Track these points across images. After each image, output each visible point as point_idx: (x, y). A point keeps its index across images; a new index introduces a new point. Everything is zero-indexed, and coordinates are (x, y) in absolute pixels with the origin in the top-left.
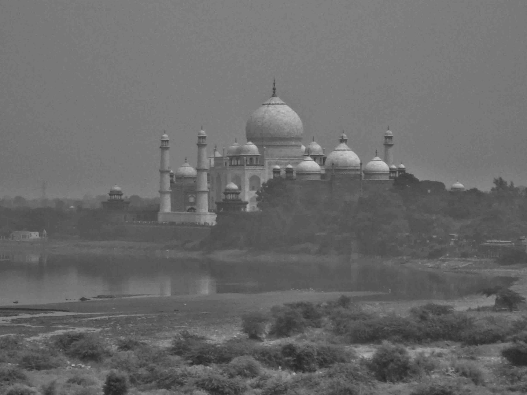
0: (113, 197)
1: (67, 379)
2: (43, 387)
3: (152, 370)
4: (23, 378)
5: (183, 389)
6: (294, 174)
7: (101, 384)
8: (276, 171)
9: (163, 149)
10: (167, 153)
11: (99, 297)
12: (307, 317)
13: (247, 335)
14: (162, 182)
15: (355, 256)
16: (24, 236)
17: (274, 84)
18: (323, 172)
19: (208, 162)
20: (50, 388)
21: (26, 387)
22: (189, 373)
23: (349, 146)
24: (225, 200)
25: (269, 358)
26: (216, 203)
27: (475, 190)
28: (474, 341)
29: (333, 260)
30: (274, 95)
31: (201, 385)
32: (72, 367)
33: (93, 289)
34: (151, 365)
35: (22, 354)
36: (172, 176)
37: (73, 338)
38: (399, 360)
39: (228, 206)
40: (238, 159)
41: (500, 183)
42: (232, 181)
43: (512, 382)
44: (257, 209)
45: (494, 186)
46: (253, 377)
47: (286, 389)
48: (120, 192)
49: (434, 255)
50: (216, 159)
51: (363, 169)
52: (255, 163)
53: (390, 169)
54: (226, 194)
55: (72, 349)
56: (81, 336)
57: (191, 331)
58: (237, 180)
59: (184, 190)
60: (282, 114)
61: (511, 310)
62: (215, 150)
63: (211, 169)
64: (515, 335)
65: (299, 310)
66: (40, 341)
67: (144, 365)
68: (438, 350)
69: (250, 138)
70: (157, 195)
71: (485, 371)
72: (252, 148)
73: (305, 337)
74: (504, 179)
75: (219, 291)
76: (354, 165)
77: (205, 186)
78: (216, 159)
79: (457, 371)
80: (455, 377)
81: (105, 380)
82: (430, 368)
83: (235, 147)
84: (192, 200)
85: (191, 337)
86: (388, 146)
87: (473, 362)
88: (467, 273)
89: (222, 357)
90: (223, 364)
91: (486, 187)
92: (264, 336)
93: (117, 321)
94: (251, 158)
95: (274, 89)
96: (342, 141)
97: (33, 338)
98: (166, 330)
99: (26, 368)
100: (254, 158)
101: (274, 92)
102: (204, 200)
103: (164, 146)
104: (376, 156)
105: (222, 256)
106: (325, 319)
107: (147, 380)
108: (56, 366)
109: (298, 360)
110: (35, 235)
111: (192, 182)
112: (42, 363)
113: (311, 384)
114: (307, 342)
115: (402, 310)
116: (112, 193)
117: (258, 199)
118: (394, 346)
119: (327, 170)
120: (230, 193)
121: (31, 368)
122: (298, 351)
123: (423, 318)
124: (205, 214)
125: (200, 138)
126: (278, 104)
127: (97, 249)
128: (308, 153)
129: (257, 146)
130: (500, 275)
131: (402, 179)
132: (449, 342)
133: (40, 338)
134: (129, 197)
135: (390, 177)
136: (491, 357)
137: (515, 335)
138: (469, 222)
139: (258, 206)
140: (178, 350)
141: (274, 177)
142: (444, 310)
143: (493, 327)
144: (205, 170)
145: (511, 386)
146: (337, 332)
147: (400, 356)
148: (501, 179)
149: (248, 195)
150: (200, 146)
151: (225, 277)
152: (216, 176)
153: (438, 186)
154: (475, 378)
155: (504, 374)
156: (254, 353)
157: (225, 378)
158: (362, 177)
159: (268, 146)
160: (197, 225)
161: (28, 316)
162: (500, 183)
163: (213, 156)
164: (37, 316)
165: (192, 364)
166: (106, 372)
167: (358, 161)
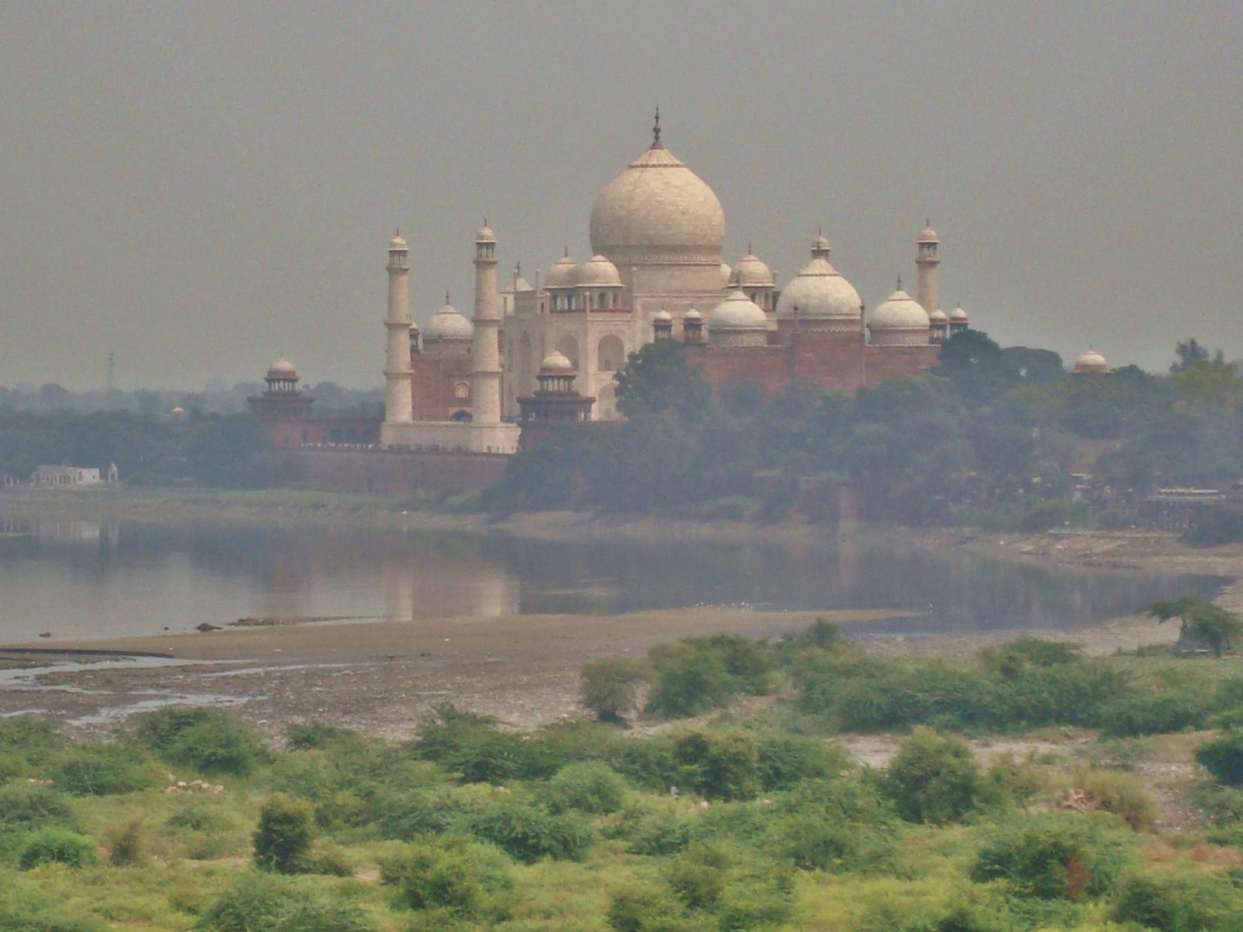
0: (276, 387)
1: (166, 816)
2: (110, 834)
3: (369, 794)
4: (61, 814)
5: (443, 840)
6: (704, 332)
7: (249, 826)
8: (661, 326)
10: (403, 279)
11: (241, 622)
13: (594, 714)
14: (390, 351)
15: (847, 526)
16: (65, 479)
17: (657, 118)
18: (773, 327)
19: (500, 304)
20: (128, 838)
21: (72, 835)
22: (456, 803)
23: (835, 265)
24: (542, 394)
25: (646, 768)
26: (520, 400)
27: (1132, 369)
28: (1127, 727)
29: (796, 534)
30: (656, 145)
31: (485, 831)
32: (178, 787)
34: (367, 783)
35: (65, 756)
36: (414, 335)
37: (182, 720)
38: (953, 772)
40: (571, 297)
41: (1191, 352)
42: (557, 349)
43: (1219, 823)
44: (616, 415)
45: (1179, 360)
46: (607, 811)
47: (685, 840)
48: (292, 373)
49: (1034, 524)
50: (519, 296)
51: (866, 321)
52: (611, 307)
53: (932, 320)
54: (541, 378)
55: (179, 746)
56: (199, 715)
57: (460, 704)
58: (570, 346)
59: (442, 370)
60: (676, 190)
61: (1217, 655)
62: (517, 275)
63: (507, 318)
64: (1226, 713)
65: (716, 654)
66: (103, 727)
67: (350, 783)
68: (1044, 748)
69: (601, 247)
70: (381, 382)
71: (1155, 798)
72: (605, 270)
73: (726, 717)
74: (1200, 343)
75: (524, 609)
76: (845, 310)
77: (492, 359)
78: (519, 296)
79: (1090, 796)
80: (1083, 813)
81: (259, 819)
82: (1026, 791)
83: (563, 267)
84: (461, 393)
85: (460, 717)
86: (925, 265)
87: (1124, 778)
88: (1115, 565)
90: (538, 781)
91: (1158, 360)
92: (633, 714)
93: (284, 679)
94: (603, 293)
95: (657, 131)
96: (818, 253)
97: (86, 720)
98: (403, 702)
99: (71, 789)
100: (610, 295)
101: (657, 138)
102: (491, 394)
103: (396, 264)
104: (899, 289)
105: (536, 525)
106: (778, 675)
107: (356, 820)
108: (141, 786)
109: (713, 773)
110: (90, 476)
112: (112, 778)
113: (745, 828)
115: (961, 653)
116: (274, 376)
117: (618, 392)
118: (940, 740)
119: (780, 322)
120: (553, 378)
121: (84, 791)
122: (714, 751)
123: (1009, 672)
124: (492, 427)
125: (480, 245)
126: (666, 166)
127: (237, 508)
128: (737, 282)
129: (617, 265)
130: (1194, 570)
131: (960, 345)
134: (312, 386)
135: (932, 340)
136: (1170, 765)
137: (1226, 713)
139: (619, 407)
140: (431, 747)
141: (656, 339)
142: (1058, 654)
144: (494, 321)
146: (807, 704)
147: (952, 760)
148: (1193, 343)
149: (596, 382)
150: (482, 264)
151: (540, 575)
152: (519, 337)
153: (1049, 359)
154: (1134, 815)
155: (1202, 805)
156: (609, 755)
157: (541, 814)
158: (863, 341)
159: (642, 266)
160: (474, 454)
161: (74, 667)
162: (1191, 352)
163: (510, 288)
164: (97, 666)
165: (463, 781)
166: (258, 799)
167: (856, 301)
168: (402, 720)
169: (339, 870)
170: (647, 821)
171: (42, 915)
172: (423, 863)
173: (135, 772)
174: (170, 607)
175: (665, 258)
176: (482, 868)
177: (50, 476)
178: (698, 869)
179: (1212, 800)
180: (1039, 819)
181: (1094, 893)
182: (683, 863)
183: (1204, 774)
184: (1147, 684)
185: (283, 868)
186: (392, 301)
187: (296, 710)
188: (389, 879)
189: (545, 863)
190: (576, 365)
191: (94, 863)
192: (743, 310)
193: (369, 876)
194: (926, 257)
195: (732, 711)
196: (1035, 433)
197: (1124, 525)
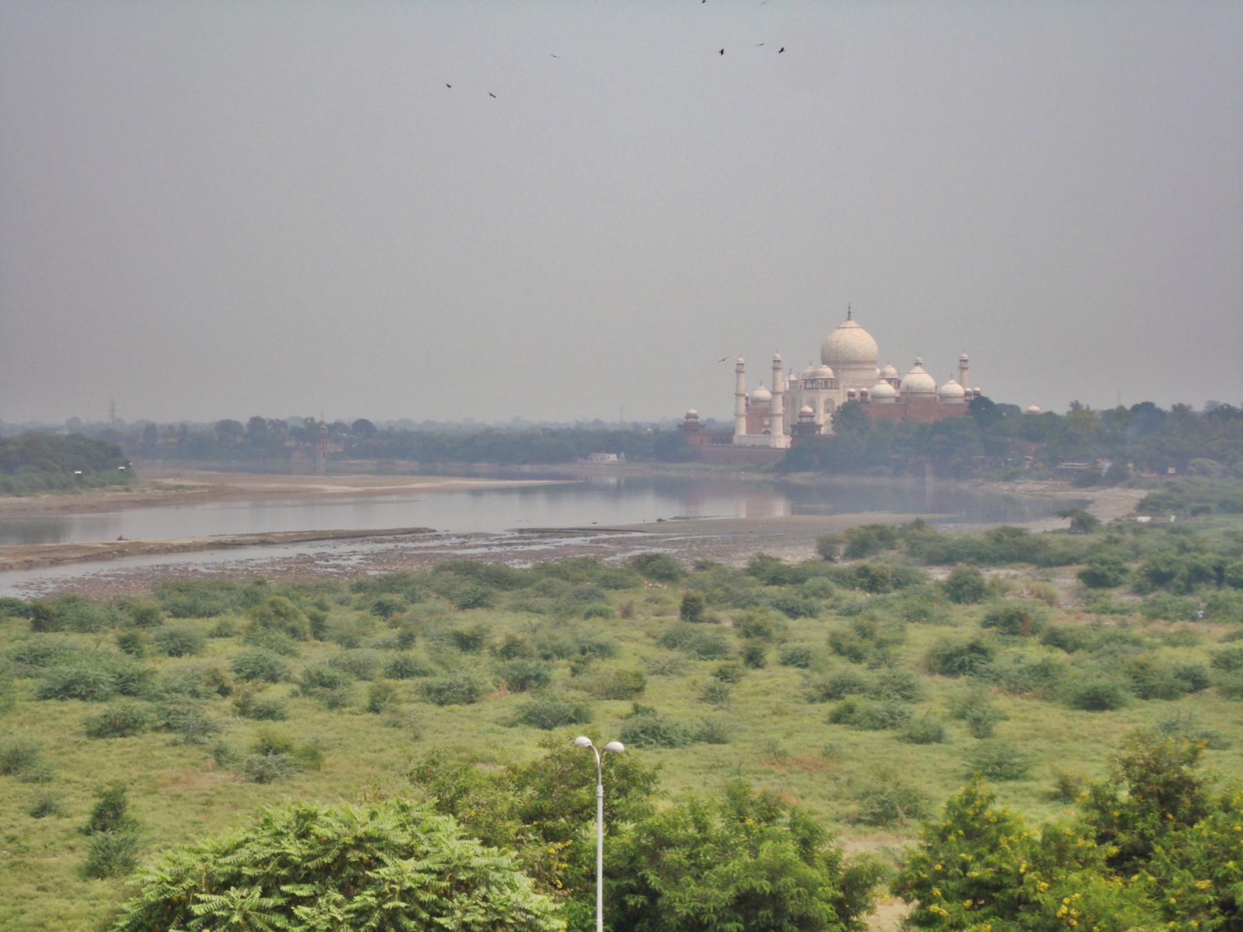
3: (727, 590)
5: (758, 609)
6: (869, 398)
7: (677, 603)
8: (851, 395)
9: (738, 372)
10: (742, 376)
12: (881, 539)
13: (821, 557)
15: (929, 479)
19: (783, 386)
21: (604, 606)
22: (764, 595)
28: (1048, 563)
31: (777, 606)
33: (668, 510)
34: (727, 585)
35: (601, 573)
36: (747, 399)
39: (803, 429)
40: (812, 382)
41: (1076, 406)
44: (832, 432)
49: (1006, 479)
50: (791, 382)
54: (801, 416)
57: (766, 552)
58: (812, 403)
59: (759, 413)
60: (856, 338)
63: (787, 392)
68: (1013, 572)
69: (825, 361)
72: (827, 371)
73: (880, 559)
74: (1080, 402)
75: (793, 513)
77: (779, 409)
78: (791, 382)
79: (1032, 592)
80: (1030, 599)
82: (1005, 590)
83: (809, 370)
84: (767, 423)
86: (963, 369)
89: (796, 577)
91: (1062, 410)
94: (826, 381)
96: (917, 364)
102: (779, 424)
107: (722, 600)
109: (873, 582)
110: (613, 457)
111: (767, 405)
114: (882, 564)
115: (976, 531)
116: (688, 416)
118: (968, 568)
128: (883, 376)
131: (978, 404)
132: (1023, 564)
133: (618, 558)
138: (1045, 445)
142: (1019, 532)
143: (1068, 549)
145: (1085, 608)
146: (912, 554)
149: (823, 419)
150: (775, 369)
152: (791, 400)
153: (1014, 409)
154: (1051, 600)
155: (1077, 597)
156: (827, 575)
157: (800, 598)
161: (605, 536)
162: (1076, 406)
166: (682, 592)
168: (741, 559)
169: (713, 620)
170: (844, 602)
171: (593, 639)
172: (750, 619)
173: (631, 579)
174: (645, 511)
175: (854, 366)
176: (774, 621)
177: (596, 457)
178: (866, 622)
179: (1085, 594)
180: (1010, 601)
181: (1033, 633)
182: (859, 619)
183: (1082, 585)
184: (1057, 544)
185: (692, 620)
186: (738, 384)
187: (698, 554)
188: (736, 625)
189: (801, 620)
190: (815, 411)
191: (614, 617)
192: (885, 388)
193: (728, 624)
194: (963, 365)
195: (881, 556)
196: (1009, 440)
197: (1047, 479)
